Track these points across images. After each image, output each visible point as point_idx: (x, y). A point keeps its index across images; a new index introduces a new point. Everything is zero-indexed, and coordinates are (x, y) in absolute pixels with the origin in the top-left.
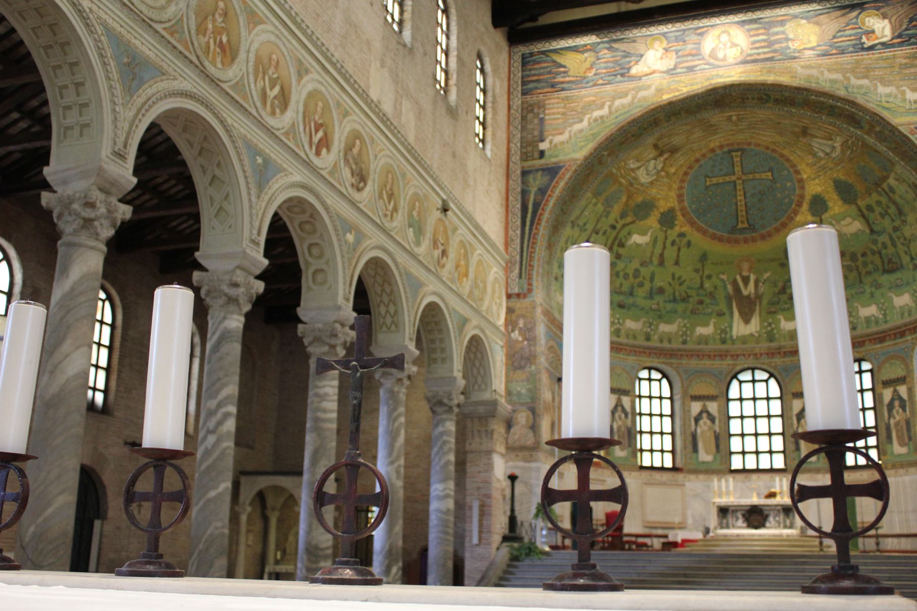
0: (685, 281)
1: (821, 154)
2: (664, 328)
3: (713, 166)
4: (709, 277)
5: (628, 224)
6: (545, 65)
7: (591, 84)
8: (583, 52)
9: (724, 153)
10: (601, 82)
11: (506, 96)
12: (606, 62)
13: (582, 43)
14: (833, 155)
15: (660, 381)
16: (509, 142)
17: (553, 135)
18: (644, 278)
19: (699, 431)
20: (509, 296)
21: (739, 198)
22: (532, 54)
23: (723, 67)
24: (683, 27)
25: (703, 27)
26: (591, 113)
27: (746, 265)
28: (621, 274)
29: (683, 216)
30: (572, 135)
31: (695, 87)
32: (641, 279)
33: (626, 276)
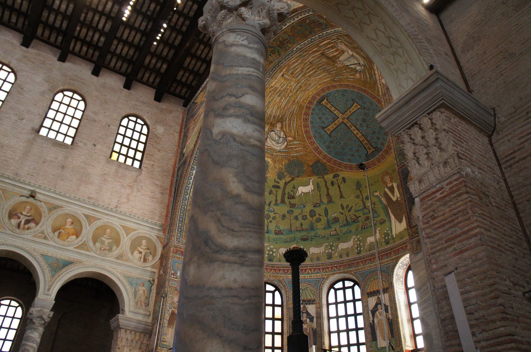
0: (352, 206)
1: (358, 68)
2: (343, 246)
3: (320, 118)
4: (367, 198)
5: (289, 182)
9: (317, 106)
14: (362, 62)
15: (352, 288)
18: (319, 215)
19: (376, 321)
20: (164, 247)
21: (355, 132)
27: (387, 179)
28: (300, 217)
29: (329, 162)
32: (317, 216)
33: (304, 218)
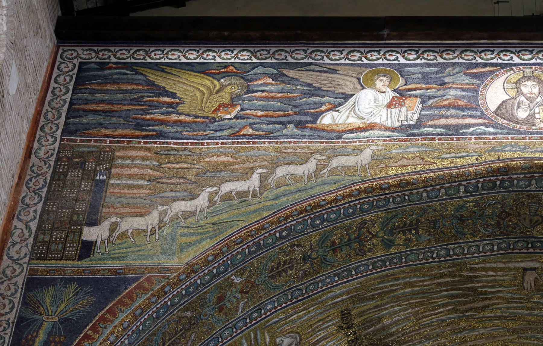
6: (130, 87)
7: (226, 133)
8: (217, 76)
10: (250, 131)
11: (26, 126)
12: (267, 98)
13: (218, 60)
16: (10, 218)
17: (123, 216)
22: (102, 66)
23: (525, 133)
24: (440, 60)
25: (485, 65)
26: (219, 185)
30: (165, 220)
31: (461, 162)
